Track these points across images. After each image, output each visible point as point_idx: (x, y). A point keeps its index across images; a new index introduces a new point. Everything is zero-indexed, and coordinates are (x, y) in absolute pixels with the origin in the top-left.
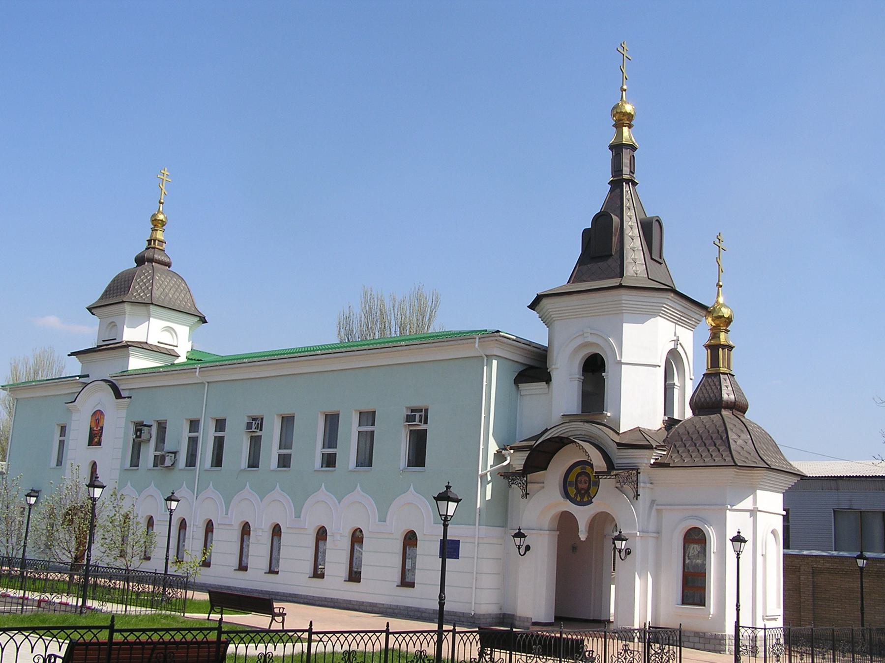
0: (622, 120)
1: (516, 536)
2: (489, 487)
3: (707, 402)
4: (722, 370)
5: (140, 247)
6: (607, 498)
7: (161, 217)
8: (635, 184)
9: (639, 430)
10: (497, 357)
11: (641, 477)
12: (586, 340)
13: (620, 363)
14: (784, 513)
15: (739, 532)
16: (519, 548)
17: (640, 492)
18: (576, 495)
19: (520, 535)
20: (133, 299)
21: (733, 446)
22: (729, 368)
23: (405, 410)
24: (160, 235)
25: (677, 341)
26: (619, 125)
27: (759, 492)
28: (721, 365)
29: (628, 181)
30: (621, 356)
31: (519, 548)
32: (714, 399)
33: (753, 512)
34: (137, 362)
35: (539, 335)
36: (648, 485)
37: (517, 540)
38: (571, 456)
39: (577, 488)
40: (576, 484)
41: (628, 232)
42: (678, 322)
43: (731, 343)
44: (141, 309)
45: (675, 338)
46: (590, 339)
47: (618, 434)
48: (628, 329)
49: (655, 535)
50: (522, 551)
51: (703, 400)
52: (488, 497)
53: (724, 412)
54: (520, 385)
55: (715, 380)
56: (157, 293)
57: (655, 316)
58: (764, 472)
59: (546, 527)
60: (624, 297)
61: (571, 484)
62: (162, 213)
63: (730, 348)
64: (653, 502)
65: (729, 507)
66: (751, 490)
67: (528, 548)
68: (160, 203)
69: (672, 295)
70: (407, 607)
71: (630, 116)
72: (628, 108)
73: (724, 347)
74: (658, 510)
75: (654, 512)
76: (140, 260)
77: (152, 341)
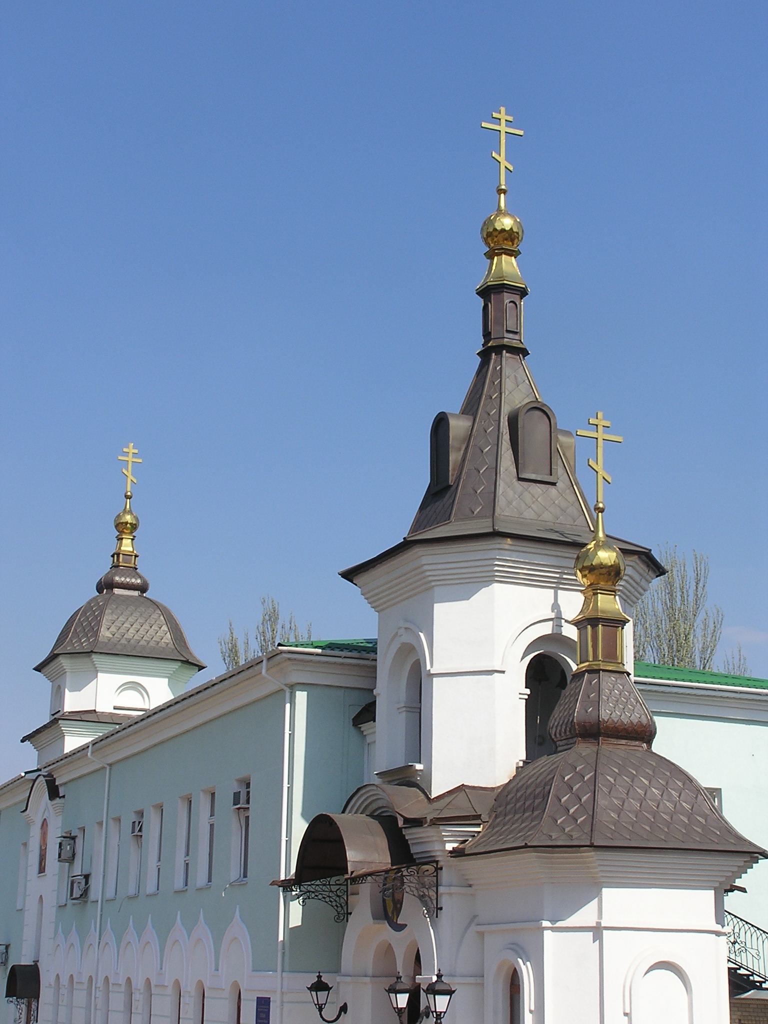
0: (500, 243)
5: (102, 569)
7: (128, 518)
9: (462, 788)
10: (303, 686)
11: (445, 875)
16: (320, 1009)
17: (444, 902)
18: (393, 913)
23: (235, 783)
24: (127, 546)
27: (605, 891)
31: (320, 1009)
33: (597, 931)
34: (73, 742)
44: (81, 662)
45: (553, 615)
46: (406, 638)
47: (429, 799)
48: (446, 614)
50: (330, 1012)
52: (296, 919)
54: (364, 727)
56: (105, 633)
57: (488, 579)
58: (592, 856)
59: (370, 972)
60: (424, 560)
62: (130, 512)
65: (546, 924)
66: (591, 889)
67: (344, 1009)
68: (127, 497)
71: (511, 235)
72: (507, 223)
74: (478, 932)
76: (100, 589)
77: (105, 706)
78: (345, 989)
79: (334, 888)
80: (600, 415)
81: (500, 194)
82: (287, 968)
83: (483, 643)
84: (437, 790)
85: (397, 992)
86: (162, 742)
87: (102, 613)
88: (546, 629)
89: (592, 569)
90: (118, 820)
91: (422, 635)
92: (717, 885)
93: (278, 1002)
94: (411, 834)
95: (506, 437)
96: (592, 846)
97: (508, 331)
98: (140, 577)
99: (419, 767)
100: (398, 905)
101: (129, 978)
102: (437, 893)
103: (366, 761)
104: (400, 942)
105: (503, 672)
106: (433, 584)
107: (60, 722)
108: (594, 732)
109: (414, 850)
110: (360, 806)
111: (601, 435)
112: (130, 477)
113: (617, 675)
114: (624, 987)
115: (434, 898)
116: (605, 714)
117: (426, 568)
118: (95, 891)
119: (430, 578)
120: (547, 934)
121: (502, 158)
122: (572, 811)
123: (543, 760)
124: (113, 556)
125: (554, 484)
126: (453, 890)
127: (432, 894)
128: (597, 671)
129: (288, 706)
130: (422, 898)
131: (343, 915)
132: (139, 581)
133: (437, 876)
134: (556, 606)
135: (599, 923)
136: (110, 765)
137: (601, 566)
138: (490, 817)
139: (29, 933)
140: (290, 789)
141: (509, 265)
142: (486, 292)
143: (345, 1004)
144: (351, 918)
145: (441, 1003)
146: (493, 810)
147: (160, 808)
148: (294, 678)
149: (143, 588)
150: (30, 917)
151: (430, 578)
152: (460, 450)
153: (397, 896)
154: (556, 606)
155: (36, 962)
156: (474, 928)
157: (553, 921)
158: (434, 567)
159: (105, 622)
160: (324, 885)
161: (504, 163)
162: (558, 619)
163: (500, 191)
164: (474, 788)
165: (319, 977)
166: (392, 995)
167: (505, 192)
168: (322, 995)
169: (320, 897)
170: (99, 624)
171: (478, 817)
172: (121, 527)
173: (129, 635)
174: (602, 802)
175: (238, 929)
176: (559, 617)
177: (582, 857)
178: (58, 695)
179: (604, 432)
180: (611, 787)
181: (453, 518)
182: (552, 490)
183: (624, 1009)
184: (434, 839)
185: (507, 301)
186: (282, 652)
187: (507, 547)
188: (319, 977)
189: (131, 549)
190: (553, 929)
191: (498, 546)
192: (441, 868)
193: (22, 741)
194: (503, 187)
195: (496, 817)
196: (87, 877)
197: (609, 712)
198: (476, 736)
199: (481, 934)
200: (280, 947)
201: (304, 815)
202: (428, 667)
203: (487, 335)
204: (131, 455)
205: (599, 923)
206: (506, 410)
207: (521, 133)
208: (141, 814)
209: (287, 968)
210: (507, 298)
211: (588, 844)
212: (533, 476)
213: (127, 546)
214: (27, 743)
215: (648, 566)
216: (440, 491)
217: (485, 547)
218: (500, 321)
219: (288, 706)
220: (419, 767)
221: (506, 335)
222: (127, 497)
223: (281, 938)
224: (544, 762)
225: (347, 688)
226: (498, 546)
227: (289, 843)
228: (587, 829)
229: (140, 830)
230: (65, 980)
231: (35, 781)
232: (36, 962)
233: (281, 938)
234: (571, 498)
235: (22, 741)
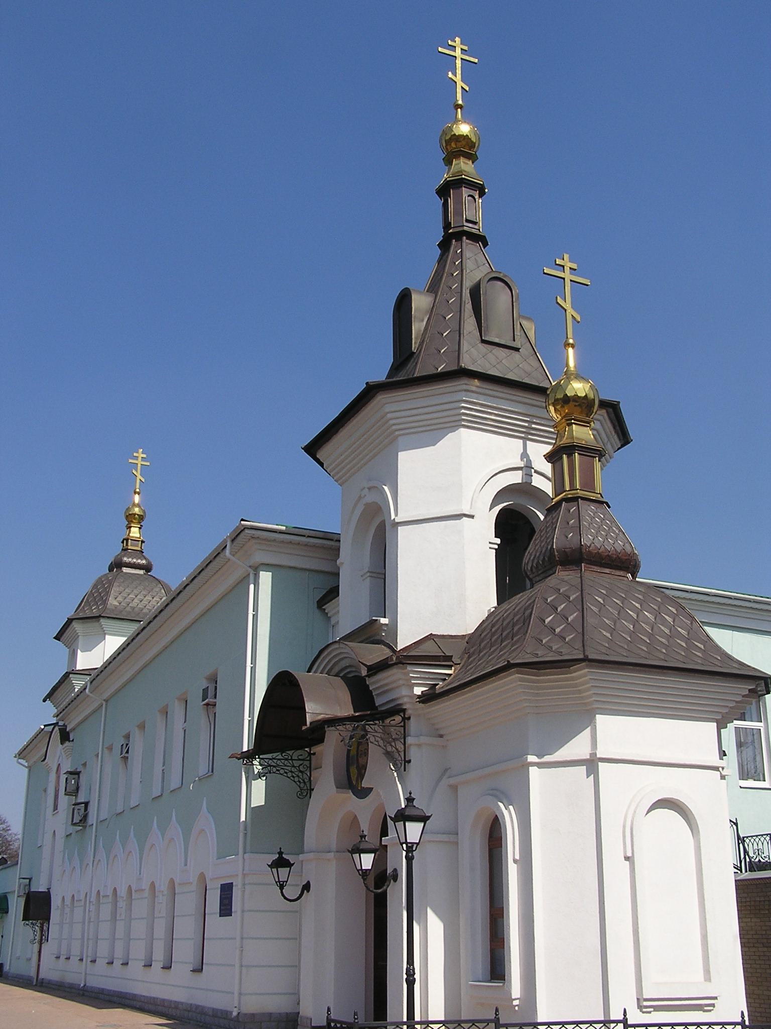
0: (458, 148)
7: (137, 510)
9: (431, 637)
10: (267, 567)
11: (413, 725)
12: (364, 501)
13: (396, 525)
16: (282, 887)
17: (414, 754)
20: (81, 615)
24: (135, 532)
27: (601, 720)
29: (460, 235)
30: (396, 515)
31: (282, 887)
33: (591, 764)
39: (358, 767)
40: (358, 760)
44: (91, 626)
46: (370, 498)
47: (394, 651)
48: (412, 464)
50: (291, 891)
54: (328, 607)
56: (112, 602)
57: (454, 424)
59: (334, 847)
60: (388, 408)
62: (138, 505)
65: (531, 758)
66: (582, 717)
67: (307, 887)
69: (476, 382)
70: (197, 1007)
72: (464, 129)
74: (450, 786)
76: (111, 569)
79: (296, 763)
80: (566, 256)
81: (457, 110)
82: (248, 847)
83: (448, 503)
84: (402, 643)
85: (361, 851)
86: (145, 666)
87: (111, 584)
88: (516, 478)
89: (566, 400)
90: (110, 749)
91: (386, 488)
92: (719, 717)
93: (239, 887)
94: (374, 683)
95: (468, 306)
96: (586, 659)
97: (467, 221)
98: (145, 558)
99: (384, 621)
100: (362, 771)
101: (115, 889)
102: (405, 744)
104: (364, 812)
105: (472, 517)
106: (397, 433)
107: (71, 676)
108: (576, 558)
109: (378, 702)
111: (567, 275)
112: (139, 477)
113: (597, 505)
114: (624, 827)
116: (587, 540)
118: (92, 819)
120: (533, 770)
122: (558, 630)
123: (516, 599)
124: (123, 542)
125: (517, 350)
126: (423, 739)
127: (400, 746)
128: (575, 499)
129: (252, 587)
130: (388, 754)
131: (306, 790)
132: (144, 562)
133: (404, 726)
134: (525, 455)
135: (593, 755)
136: (106, 701)
137: (576, 398)
138: (461, 658)
139: (45, 864)
140: (253, 670)
141: (464, 166)
142: (444, 191)
143: (308, 882)
144: (313, 793)
145: (414, 831)
146: (466, 651)
147: (142, 727)
148: (260, 557)
149: (148, 568)
150: (46, 851)
151: (394, 427)
152: (423, 321)
153: (361, 761)
154: (525, 455)
155: (49, 889)
156: (445, 782)
157: (540, 756)
158: (398, 414)
159: (114, 592)
160: (286, 759)
161: (460, 84)
162: (528, 469)
163: (458, 106)
164: (443, 636)
165: (280, 853)
166: (356, 856)
167: (461, 107)
168: (283, 872)
169: (282, 771)
170: (108, 594)
171: (449, 658)
172: (131, 519)
173: (134, 604)
174: (590, 620)
175: (205, 822)
177: (573, 679)
178: (73, 656)
179: (571, 274)
180: (601, 606)
181: (417, 373)
182: (516, 355)
183: (625, 852)
184: (401, 682)
185: (465, 195)
186: (246, 528)
187: (474, 388)
188: (280, 853)
189: (138, 535)
190: (539, 765)
191: (465, 387)
192: (409, 718)
193: (44, 701)
194: (460, 102)
195: (469, 657)
196: (86, 804)
197: (592, 539)
199: (454, 788)
200: (242, 828)
202: (393, 517)
203: (447, 225)
204: (140, 459)
205: (593, 755)
206: (468, 284)
207: (476, 61)
208: (127, 737)
209: (248, 847)
210: (465, 192)
211: (581, 656)
212: (497, 340)
213: (135, 532)
214: (48, 702)
215: (614, 428)
216: (403, 352)
217: (452, 389)
218: (459, 212)
219: (252, 587)
220: (384, 621)
221: (465, 224)
222: (135, 493)
223: (243, 818)
224: (520, 600)
226: (465, 387)
228: (578, 645)
229: (127, 752)
230: (68, 901)
231: (52, 732)
232: (49, 889)
233: (243, 818)
234: (537, 364)
235: (44, 701)
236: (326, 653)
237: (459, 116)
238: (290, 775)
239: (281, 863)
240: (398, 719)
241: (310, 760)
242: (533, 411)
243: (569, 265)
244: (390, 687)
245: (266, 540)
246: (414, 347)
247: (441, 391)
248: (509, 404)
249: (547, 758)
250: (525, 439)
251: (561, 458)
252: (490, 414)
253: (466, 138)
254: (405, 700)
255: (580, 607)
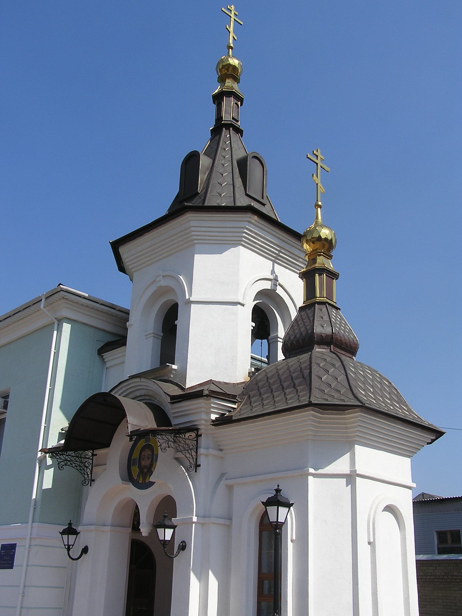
0: (228, 73)
1: (63, 533)
2: (49, 475)
3: (301, 342)
4: (318, 299)
6: (169, 476)
8: (239, 131)
9: (211, 382)
10: (69, 320)
11: (203, 441)
12: (159, 284)
13: (189, 303)
14: (414, 485)
15: (278, 491)
16: (69, 549)
17: (202, 460)
18: (138, 476)
19: (70, 531)
21: (315, 382)
22: (330, 295)
25: (275, 281)
26: (222, 80)
28: (318, 295)
29: (228, 126)
30: (190, 295)
31: (69, 549)
32: (304, 334)
33: (351, 478)
35: (119, 291)
36: (212, 451)
37: (65, 537)
38: (129, 424)
39: (140, 467)
41: (218, 168)
42: (276, 259)
43: (330, 265)
45: (272, 277)
46: (163, 283)
47: (183, 389)
49: (221, 521)
50: (76, 552)
51: (292, 337)
52: (48, 483)
53: (317, 349)
54: (106, 355)
55: (309, 312)
57: (236, 243)
60: (192, 223)
61: (134, 464)
63: (333, 275)
64: (223, 475)
65: (311, 470)
66: (346, 445)
67: (85, 550)
69: (256, 217)
72: (234, 62)
73: (322, 271)
74: (227, 486)
75: (222, 487)
78: (86, 535)
81: (229, 49)
88: (267, 285)
91: (181, 277)
93: (27, 546)
100: (147, 471)
102: (197, 452)
103: (104, 379)
105: (243, 305)
106: (195, 241)
109: (174, 422)
110: (123, 392)
114: (369, 522)
115: (195, 457)
117: (193, 229)
119: (194, 237)
120: (310, 478)
121: (231, 30)
127: (194, 454)
129: (55, 332)
133: (197, 441)
134: (273, 272)
148: (66, 313)
151: (194, 237)
152: (205, 174)
154: (273, 272)
156: (223, 482)
157: (316, 469)
160: (77, 457)
163: (230, 47)
167: (232, 48)
168: (72, 537)
176: (276, 279)
184: (203, 409)
186: (62, 290)
187: (253, 221)
190: (314, 475)
191: (249, 219)
192: (201, 435)
198: (219, 350)
199: (230, 488)
200: (33, 504)
201: (62, 408)
202: (187, 297)
207: (242, 23)
212: (254, 196)
219: (55, 332)
223: (34, 497)
225: (96, 328)
226: (249, 219)
227: (47, 429)
233: (34, 497)
236: (125, 384)
237: (231, 53)
238: (78, 468)
239: (70, 531)
240: (193, 434)
241: (92, 459)
242: (283, 244)
243: (320, 156)
244: (195, 411)
245: (72, 301)
246: (199, 190)
247: (232, 219)
248: (271, 236)
249: (320, 471)
250: (274, 262)
251: (314, 276)
252: (259, 240)
253: (234, 67)
254: (203, 422)
255: (343, 372)
